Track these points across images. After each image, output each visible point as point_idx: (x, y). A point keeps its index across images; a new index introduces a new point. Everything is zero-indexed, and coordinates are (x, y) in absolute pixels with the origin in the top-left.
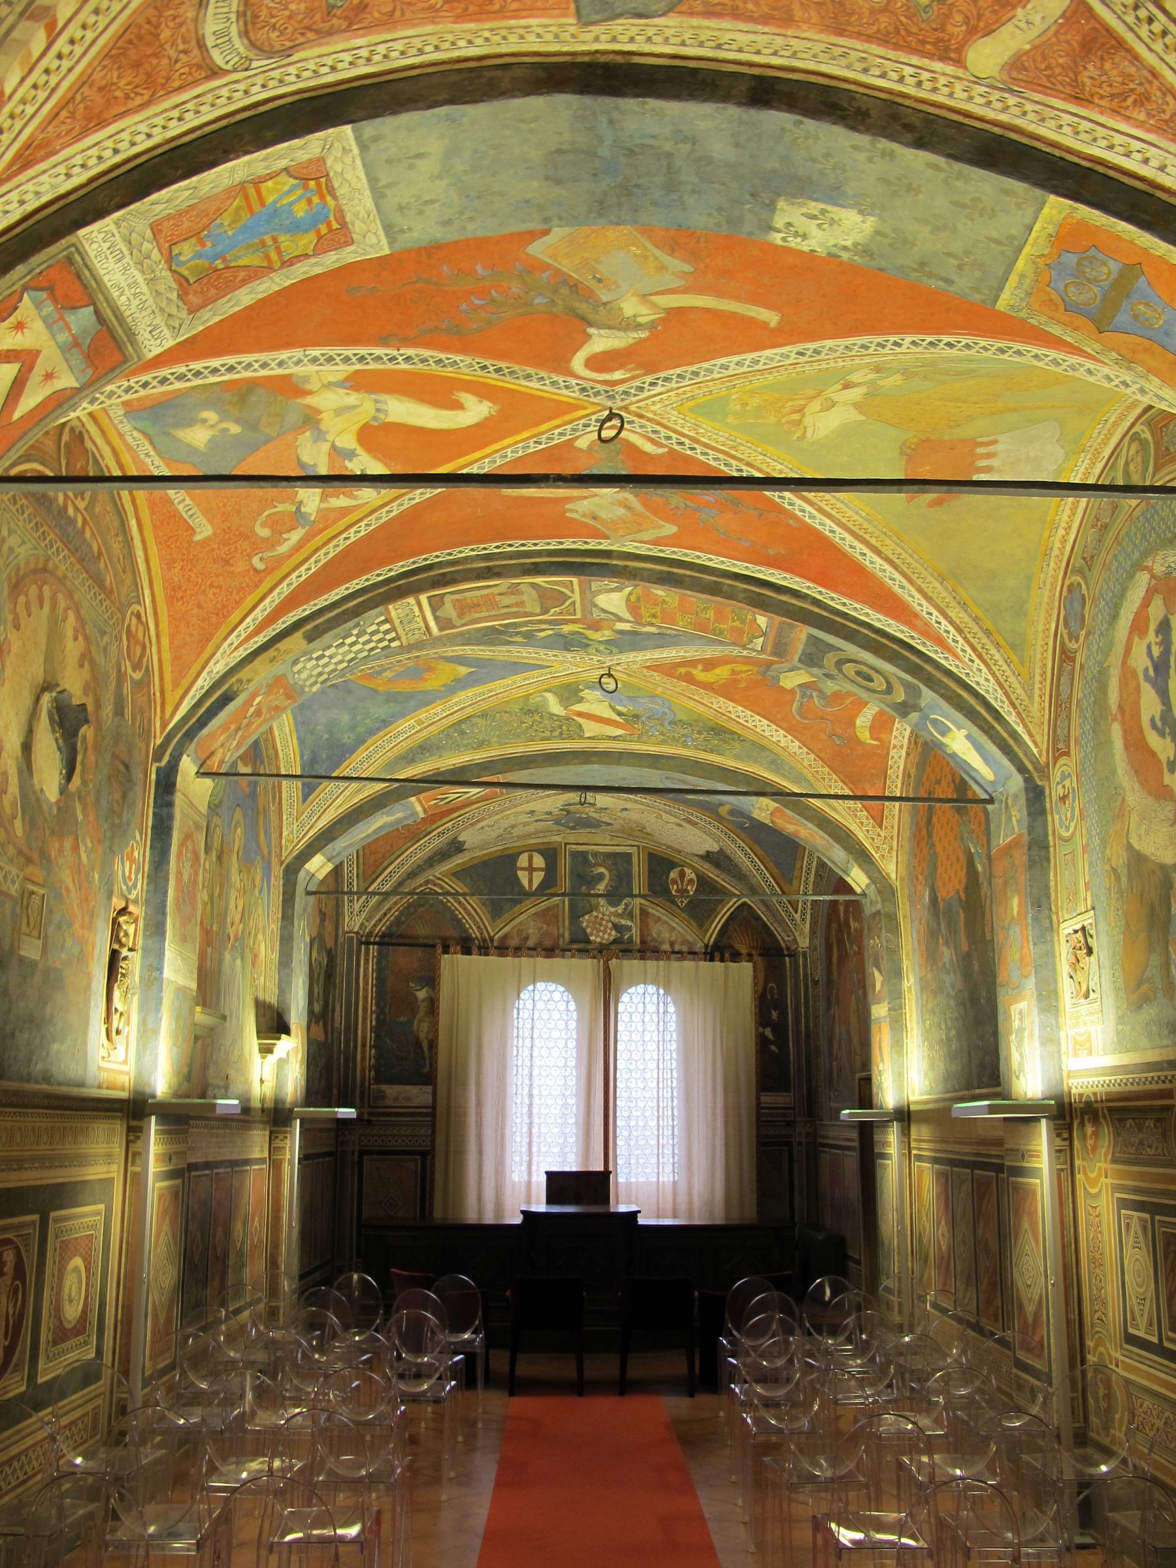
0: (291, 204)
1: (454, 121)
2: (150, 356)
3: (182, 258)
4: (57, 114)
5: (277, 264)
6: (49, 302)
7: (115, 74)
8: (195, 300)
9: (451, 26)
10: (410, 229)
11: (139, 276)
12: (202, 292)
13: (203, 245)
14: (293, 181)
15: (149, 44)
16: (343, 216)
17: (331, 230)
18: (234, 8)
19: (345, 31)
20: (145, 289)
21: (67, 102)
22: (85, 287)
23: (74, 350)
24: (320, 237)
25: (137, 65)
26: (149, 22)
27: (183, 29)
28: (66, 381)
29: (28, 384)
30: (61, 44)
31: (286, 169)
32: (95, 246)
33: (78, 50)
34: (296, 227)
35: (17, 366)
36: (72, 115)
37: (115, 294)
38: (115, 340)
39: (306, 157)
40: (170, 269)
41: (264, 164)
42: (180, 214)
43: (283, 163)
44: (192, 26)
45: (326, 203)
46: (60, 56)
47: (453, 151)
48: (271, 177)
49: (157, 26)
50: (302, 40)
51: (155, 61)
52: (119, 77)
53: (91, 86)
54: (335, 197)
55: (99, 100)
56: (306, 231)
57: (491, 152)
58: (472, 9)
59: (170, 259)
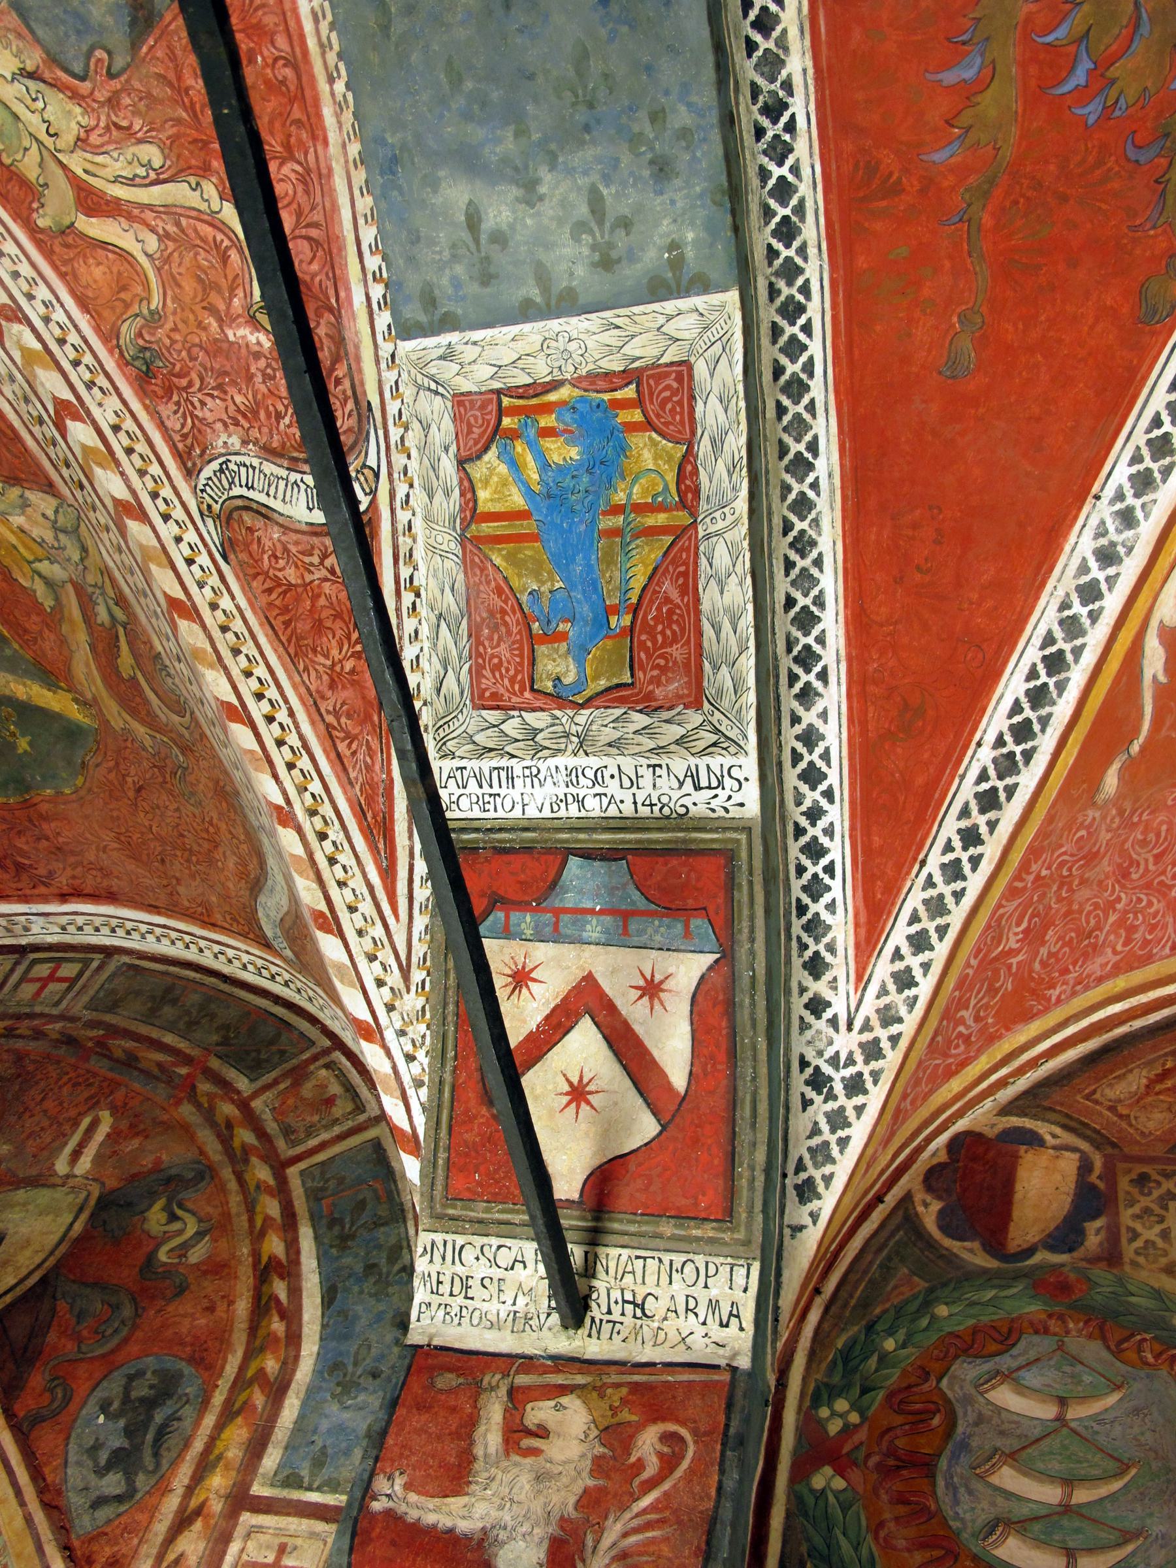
0: (545, 465)
1: (395, 160)
2: (753, 808)
3: (568, 679)
4: (339, 755)
5: (683, 518)
6: (515, 916)
7: (321, 659)
8: (675, 686)
9: (334, 149)
10: (673, 246)
11: (561, 761)
12: (663, 670)
13: (563, 636)
14: (491, 455)
15: (298, 599)
16: (608, 375)
17: (639, 402)
18: (284, 473)
19: (338, 317)
20: (594, 762)
21: (329, 736)
22: (527, 850)
23: (633, 925)
24: (649, 425)
25: (319, 627)
26: (269, 591)
27: (293, 549)
28: (687, 970)
29: (638, 1029)
30: (257, 710)
31: (461, 463)
32: (464, 803)
33: (272, 693)
34: (605, 464)
35: (586, 1023)
36: (350, 738)
37: (574, 811)
38: (668, 852)
39: (448, 424)
40: (582, 706)
41: (439, 496)
42: (477, 654)
43: (448, 466)
44: (295, 537)
45: (563, 403)
46: (270, 719)
47: (469, 162)
48: (468, 488)
49: (278, 582)
50: (347, 384)
51: (322, 601)
52: (327, 657)
53: (323, 697)
54: (554, 385)
55: (347, 694)
56: (623, 449)
57: (469, 85)
58: (297, 113)
59: (560, 699)
